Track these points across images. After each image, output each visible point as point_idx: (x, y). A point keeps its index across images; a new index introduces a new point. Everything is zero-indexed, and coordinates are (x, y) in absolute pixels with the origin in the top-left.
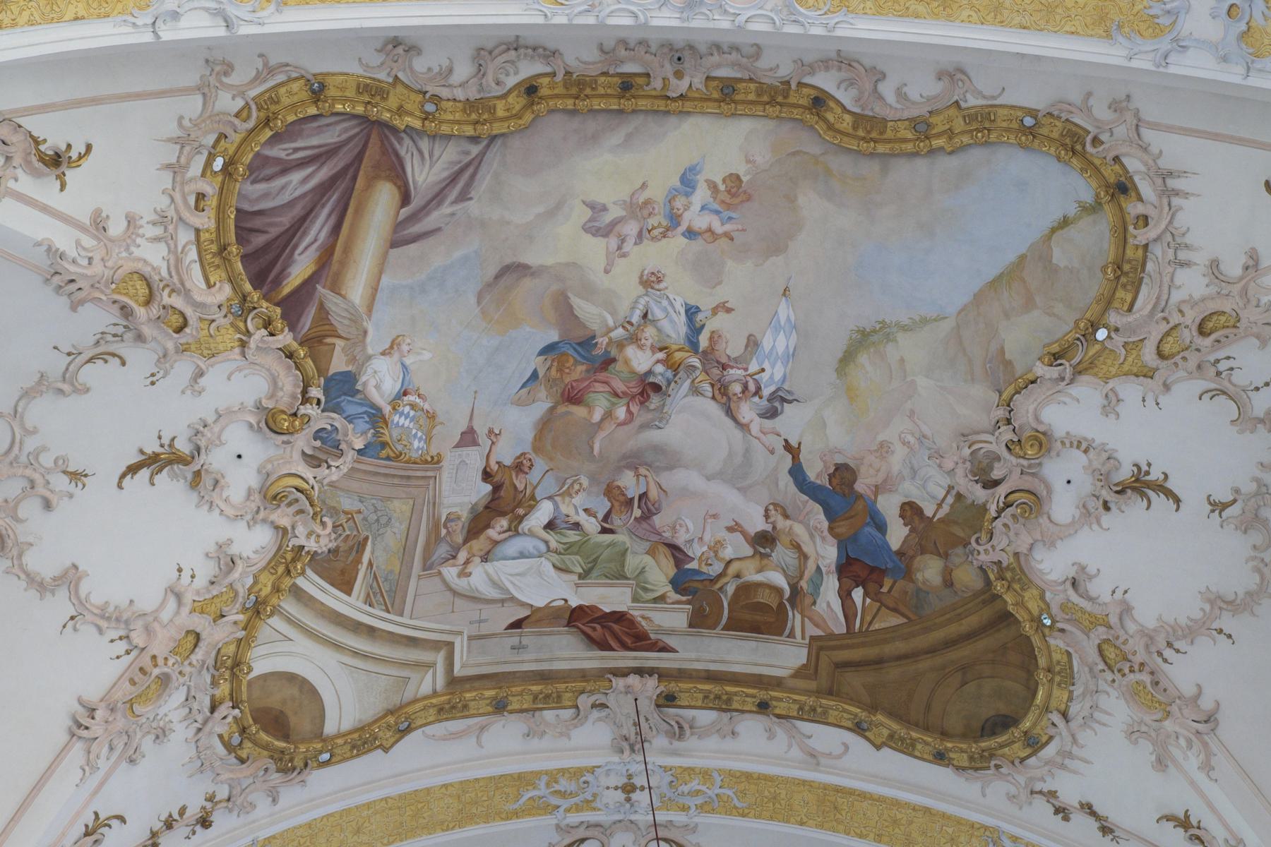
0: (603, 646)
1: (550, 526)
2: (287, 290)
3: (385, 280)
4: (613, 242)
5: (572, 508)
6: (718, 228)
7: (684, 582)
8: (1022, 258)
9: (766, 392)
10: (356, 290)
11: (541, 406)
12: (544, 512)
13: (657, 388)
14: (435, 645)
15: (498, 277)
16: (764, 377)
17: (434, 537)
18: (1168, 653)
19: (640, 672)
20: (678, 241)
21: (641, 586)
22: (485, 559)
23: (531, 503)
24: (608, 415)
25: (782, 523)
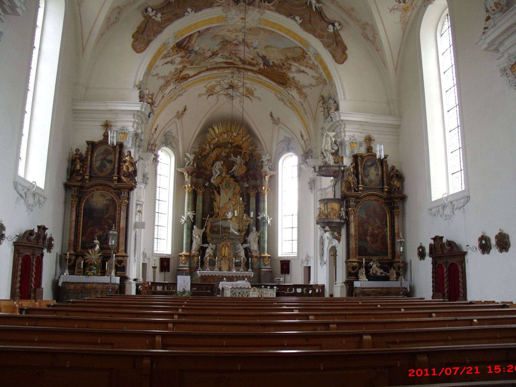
0: (228, 64)
1: (221, 56)
2: (183, 46)
3: (197, 40)
4: (231, 33)
5: (225, 54)
6: (247, 32)
7: (240, 60)
8: (291, 48)
9: (254, 47)
10: (193, 42)
11: (220, 46)
12: (221, 54)
13: (238, 45)
14: (205, 66)
15: (213, 37)
16: (254, 46)
17: (205, 58)
18: (303, 88)
19: (234, 67)
20: (241, 33)
21: (235, 60)
22: (212, 59)
23: (219, 54)
24: (230, 46)
25: (255, 58)
